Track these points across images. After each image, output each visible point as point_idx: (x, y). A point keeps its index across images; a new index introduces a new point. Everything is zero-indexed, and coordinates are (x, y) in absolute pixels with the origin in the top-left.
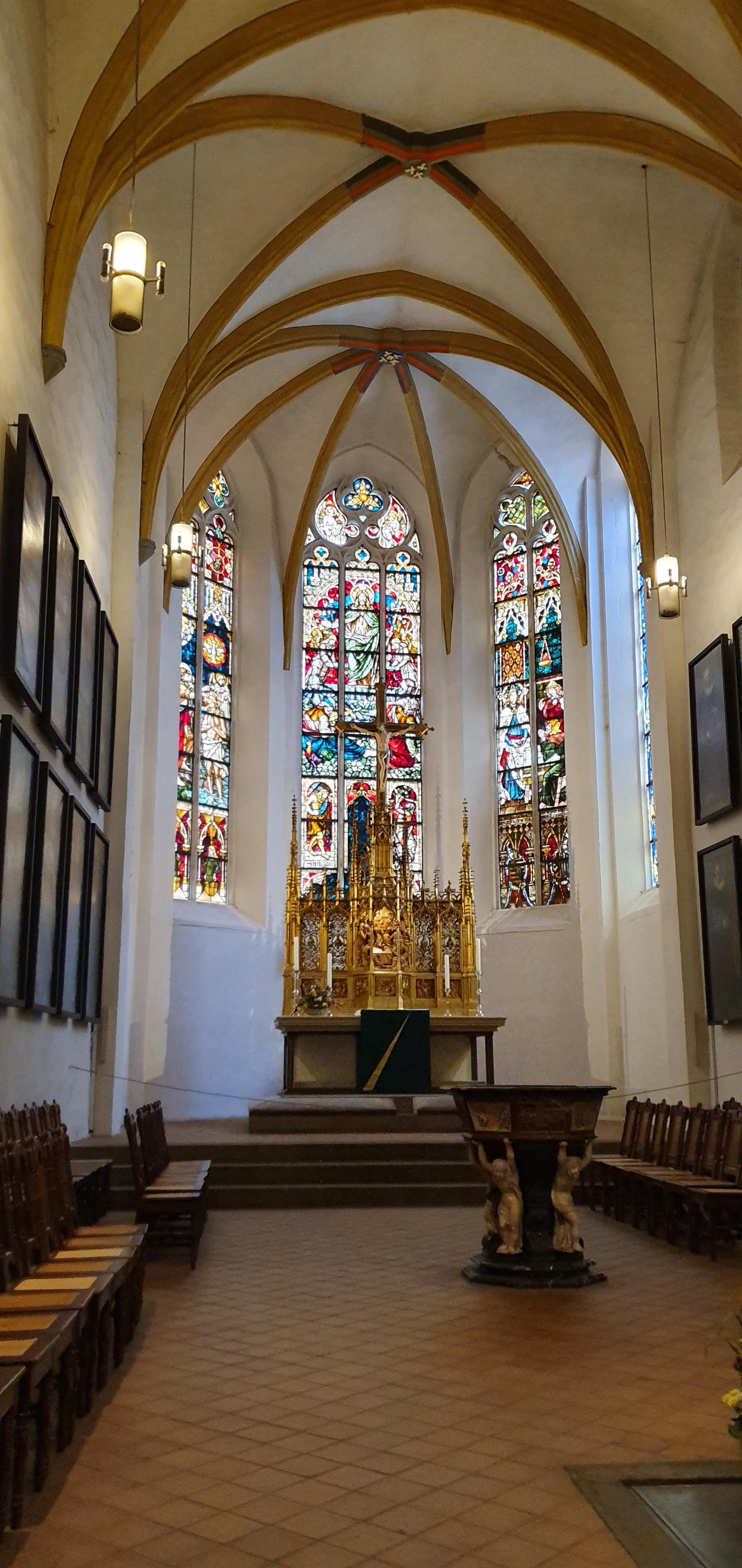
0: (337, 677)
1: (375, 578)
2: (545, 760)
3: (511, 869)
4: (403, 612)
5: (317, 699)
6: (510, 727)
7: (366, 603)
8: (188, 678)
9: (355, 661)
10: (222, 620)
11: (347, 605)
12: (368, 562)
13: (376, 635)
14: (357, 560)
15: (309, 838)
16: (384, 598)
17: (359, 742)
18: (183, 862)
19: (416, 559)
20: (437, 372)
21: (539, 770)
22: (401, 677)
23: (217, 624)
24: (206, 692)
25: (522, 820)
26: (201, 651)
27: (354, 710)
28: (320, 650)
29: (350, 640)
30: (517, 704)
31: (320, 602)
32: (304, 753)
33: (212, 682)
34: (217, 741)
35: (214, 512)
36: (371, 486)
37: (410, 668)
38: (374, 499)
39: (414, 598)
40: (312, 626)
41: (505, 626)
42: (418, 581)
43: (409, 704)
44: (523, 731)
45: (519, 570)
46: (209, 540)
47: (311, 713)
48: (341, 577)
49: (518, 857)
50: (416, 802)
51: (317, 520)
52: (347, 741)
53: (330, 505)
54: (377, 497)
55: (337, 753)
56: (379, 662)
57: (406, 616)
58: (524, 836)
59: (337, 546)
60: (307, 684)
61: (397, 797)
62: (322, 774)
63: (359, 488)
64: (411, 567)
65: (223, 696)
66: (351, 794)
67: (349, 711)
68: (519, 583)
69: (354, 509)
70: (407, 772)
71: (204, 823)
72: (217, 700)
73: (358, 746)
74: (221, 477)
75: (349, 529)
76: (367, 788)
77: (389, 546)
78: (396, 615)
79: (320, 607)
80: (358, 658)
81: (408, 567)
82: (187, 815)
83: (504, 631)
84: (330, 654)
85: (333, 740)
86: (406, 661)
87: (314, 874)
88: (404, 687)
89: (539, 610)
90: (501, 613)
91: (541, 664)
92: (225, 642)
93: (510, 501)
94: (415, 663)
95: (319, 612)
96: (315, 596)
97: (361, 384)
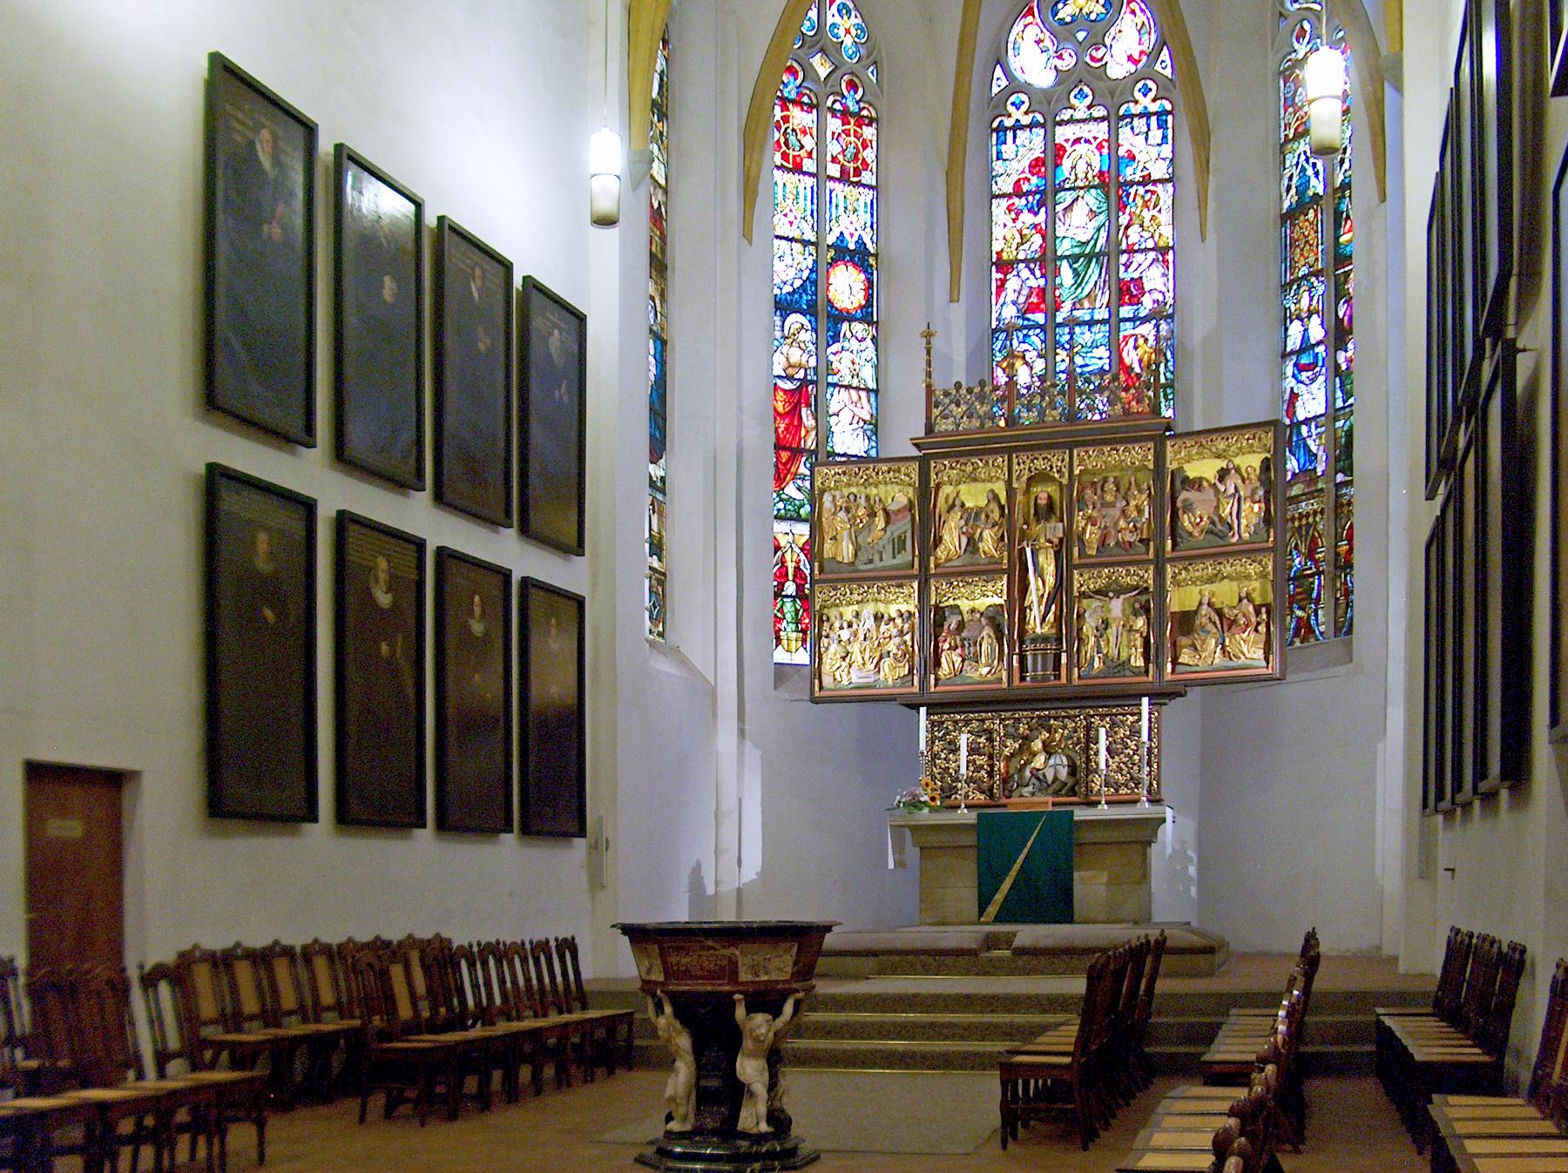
3: (1296, 583)
4: (1146, 180)
8: (806, 336)
9: (1071, 271)
11: (1057, 182)
12: (1089, 107)
13: (1104, 224)
14: (1073, 108)
21: (1336, 419)
22: (1143, 288)
24: (834, 354)
25: (1313, 505)
31: (1017, 184)
34: (857, 426)
37: (1157, 271)
40: (1005, 225)
42: (1170, 125)
48: (1049, 137)
49: (1306, 564)
57: (1150, 187)
58: (1315, 529)
59: (1043, 91)
60: (998, 320)
65: (864, 355)
69: (1067, 24)
72: (853, 363)
75: (1060, 57)
78: (1135, 187)
79: (1018, 192)
80: (1075, 266)
84: (1032, 266)
92: (865, 272)
94: (1165, 262)
95: (1016, 200)
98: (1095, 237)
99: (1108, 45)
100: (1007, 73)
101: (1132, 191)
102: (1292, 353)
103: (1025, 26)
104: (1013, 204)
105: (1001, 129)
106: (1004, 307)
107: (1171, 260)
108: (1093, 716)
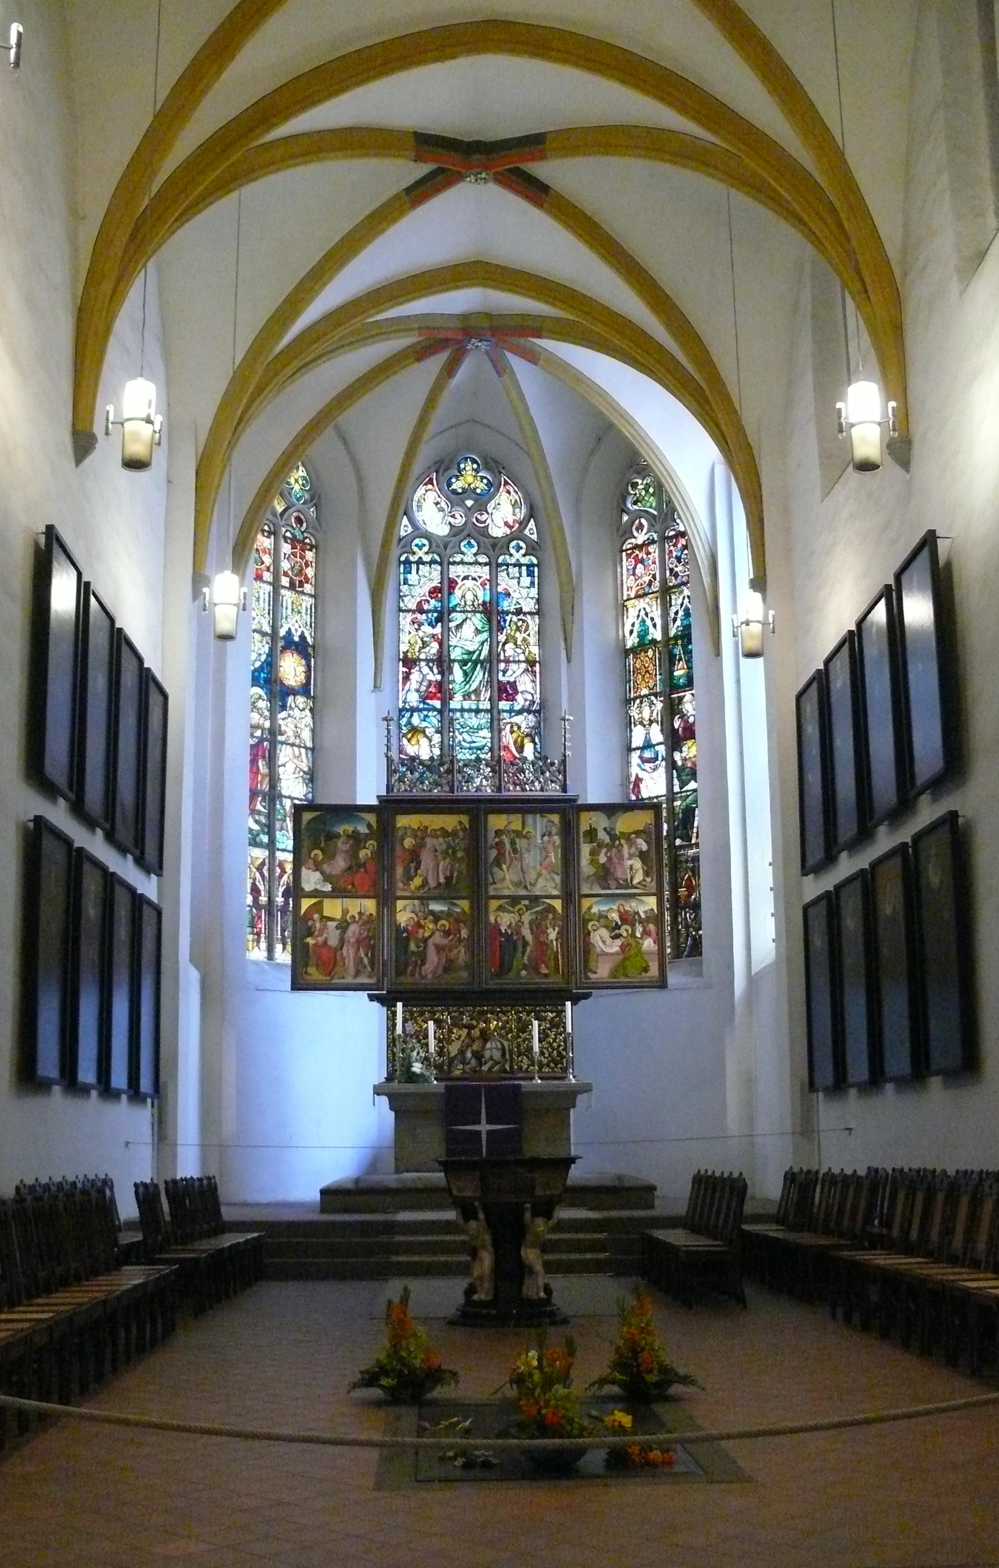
1: (485, 572)
2: (681, 788)
4: (519, 612)
5: (416, 720)
6: (642, 749)
8: (263, 704)
9: (461, 672)
10: (303, 632)
12: (475, 555)
14: (463, 553)
16: (496, 596)
18: (260, 918)
19: (533, 549)
20: (532, 357)
23: (296, 639)
24: (283, 719)
26: (277, 671)
28: (420, 660)
30: (651, 722)
31: (420, 602)
33: (290, 707)
35: (291, 510)
36: (478, 465)
41: (636, 629)
42: (536, 574)
43: (526, 721)
44: (657, 753)
45: (650, 562)
46: (286, 542)
47: (409, 736)
51: (415, 508)
56: (490, 673)
57: (521, 617)
60: (405, 702)
64: (528, 557)
65: (304, 721)
68: (650, 577)
69: (458, 494)
71: (283, 871)
72: (296, 727)
74: (301, 468)
75: (453, 516)
79: (420, 610)
82: (263, 864)
83: (635, 634)
84: (431, 664)
86: (522, 670)
88: (520, 701)
89: (674, 609)
90: (632, 614)
91: (676, 673)
93: (640, 481)
94: (534, 673)
95: (418, 615)
97: (450, 369)
100: (412, 521)
101: (508, 618)
102: (637, 749)
108: (521, 1012)
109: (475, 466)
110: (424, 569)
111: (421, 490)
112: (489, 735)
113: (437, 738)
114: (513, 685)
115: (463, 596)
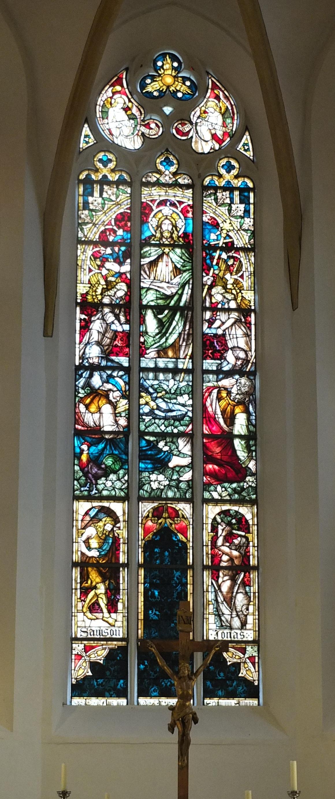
0: (128, 346)
4: (229, 247)
5: (96, 381)
7: (172, 233)
11: (143, 237)
12: (175, 174)
13: (188, 282)
15: (85, 592)
17: (161, 444)
22: (226, 345)
27: (155, 395)
29: (149, 289)
31: (104, 232)
32: (76, 462)
37: (239, 331)
38: (184, 83)
39: (245, 227)
40: (90, 270)
42: (252, 201)
47: (88, 401)
48: (135, 197)
50: (250, 536)
52: (143, 443)
53: (119, 92)
54: (189, 79)
55: (127, 461)
60: (82, 358)
61: (220, 528)
62: (105, 493)
63: (162, 67)
64: (241, 180)
66: (150, 523)
67: (146, 398)
70: (234, 490)
73: (161, 450)
75: (147, 126)
76: (175, 514)
77: (207, 149)
78: (218, 252)
79: (103, 241)
80: (160, 316)
81: (236, 181)
84: (117, 311)
85: (121, 441)
87: (93, 647)
94: (248, 325)
96: (95, 225)
98: (180, 292)
99: (194, 122)
101: (216, 255)
103: (114, 93)
104: (99, 252)
105: (88, 182)
106: (88, 347)
107: (253, 322)
109: (176, 64)
110: (109, 191)
111: (108, 92)
112: (190, 402)
113: (123, 405)
114: (222, 338)
115: (159, 226)
